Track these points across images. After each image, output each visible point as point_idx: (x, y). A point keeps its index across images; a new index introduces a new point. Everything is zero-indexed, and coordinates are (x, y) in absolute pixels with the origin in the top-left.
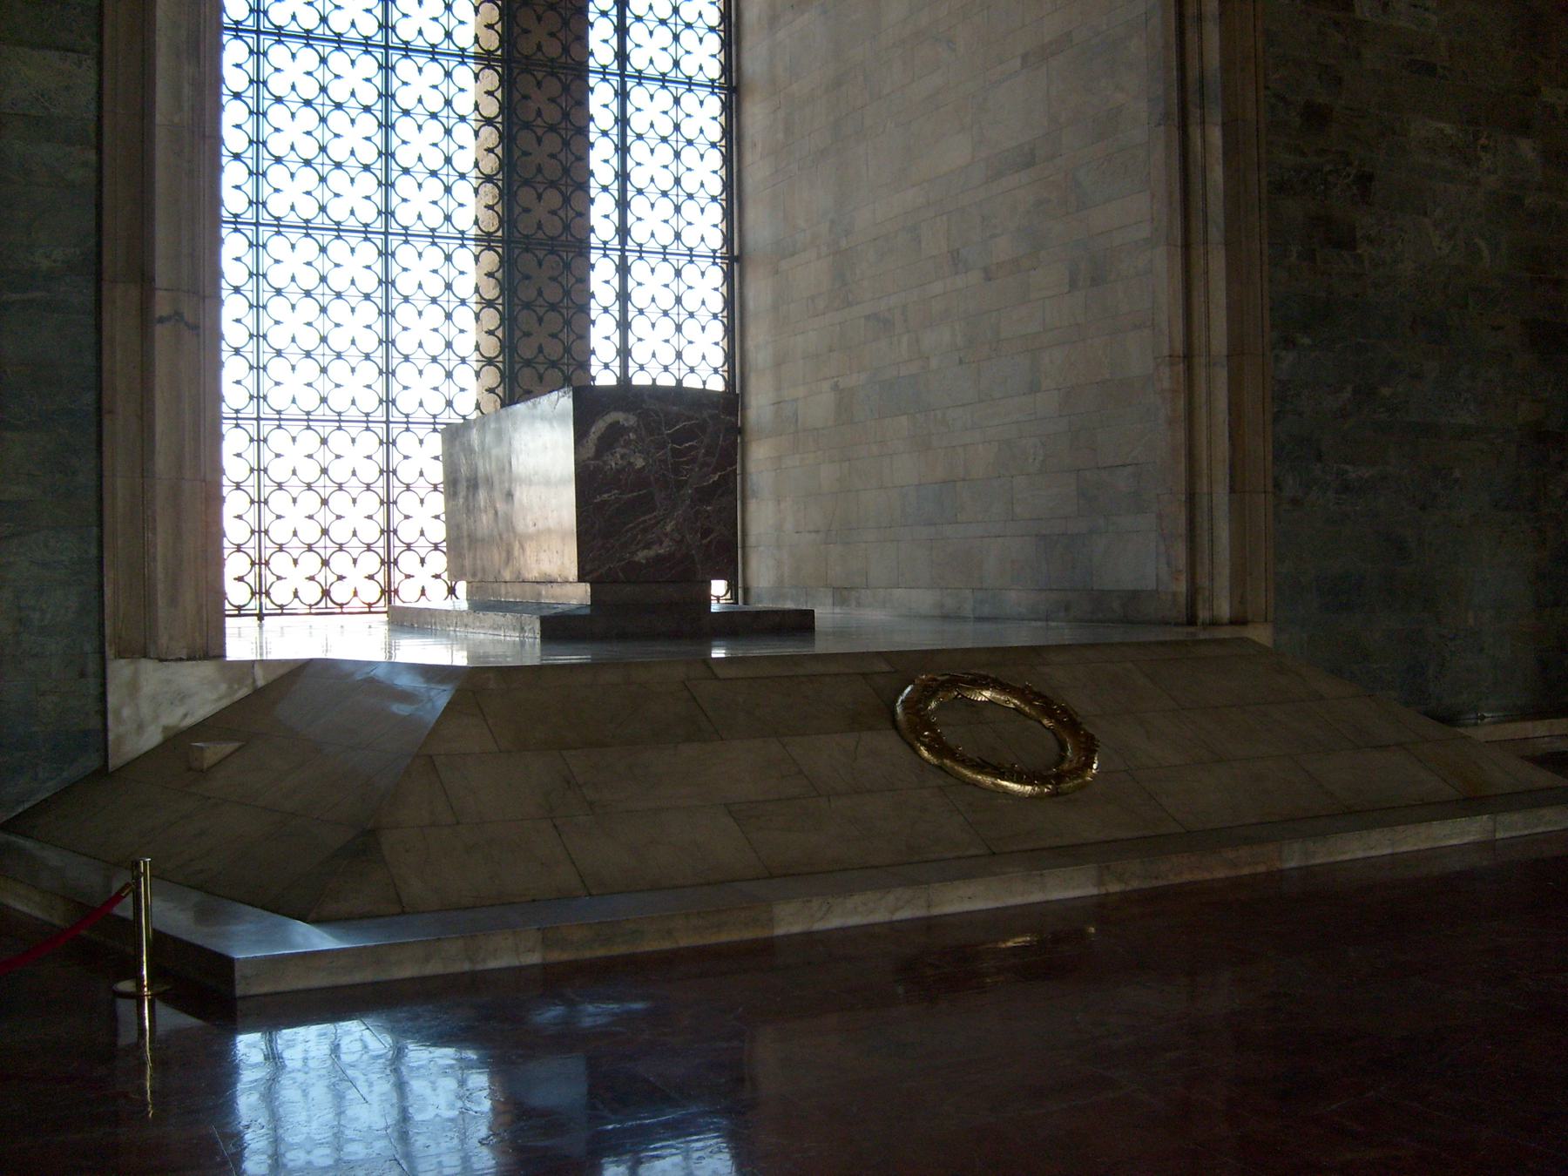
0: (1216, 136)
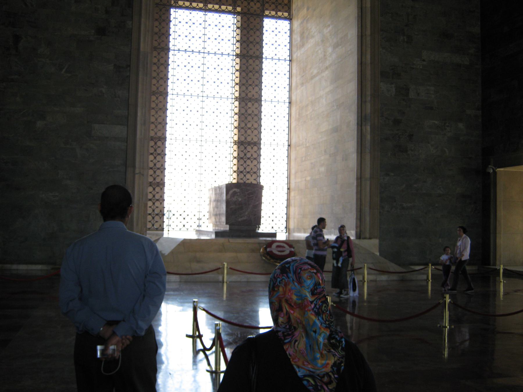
0: (368, 128)
